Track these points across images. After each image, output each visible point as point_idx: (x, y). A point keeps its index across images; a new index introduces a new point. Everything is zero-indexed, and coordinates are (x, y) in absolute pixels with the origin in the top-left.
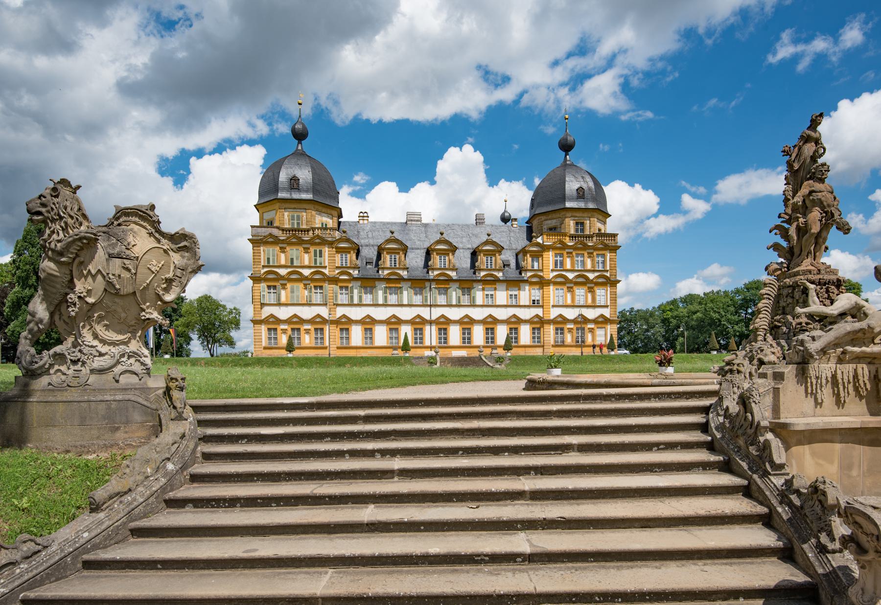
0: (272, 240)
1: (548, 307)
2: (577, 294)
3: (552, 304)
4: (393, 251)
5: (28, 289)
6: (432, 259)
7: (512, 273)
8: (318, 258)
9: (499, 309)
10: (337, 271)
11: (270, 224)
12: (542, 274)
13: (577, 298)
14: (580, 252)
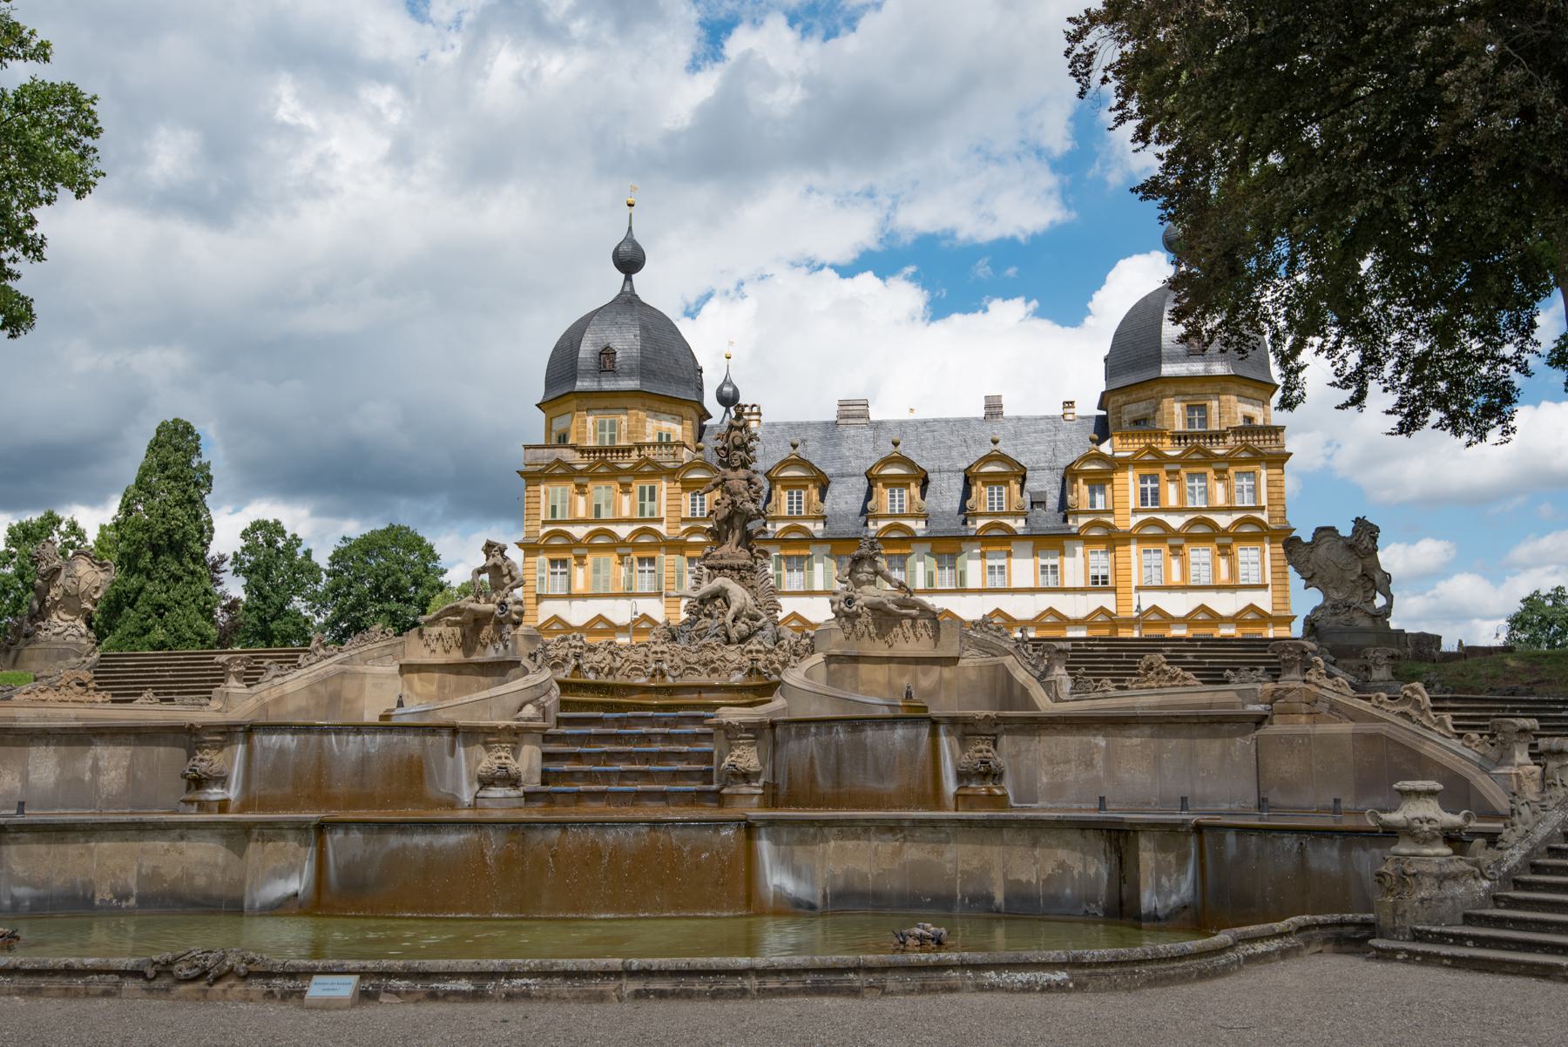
0: (562, 471)
1: (1125, 590)
2: (1192, 560)
3: (1135, 583)
5: (136, 576)
6: (875, 497)
7: (1047, 518)
8: (647, 503)
9: (1017, 597)
10: (683, 528)
11: (563, 439)
12: (1110, 520)
13: (1193, 569)
14: (1196, 470)
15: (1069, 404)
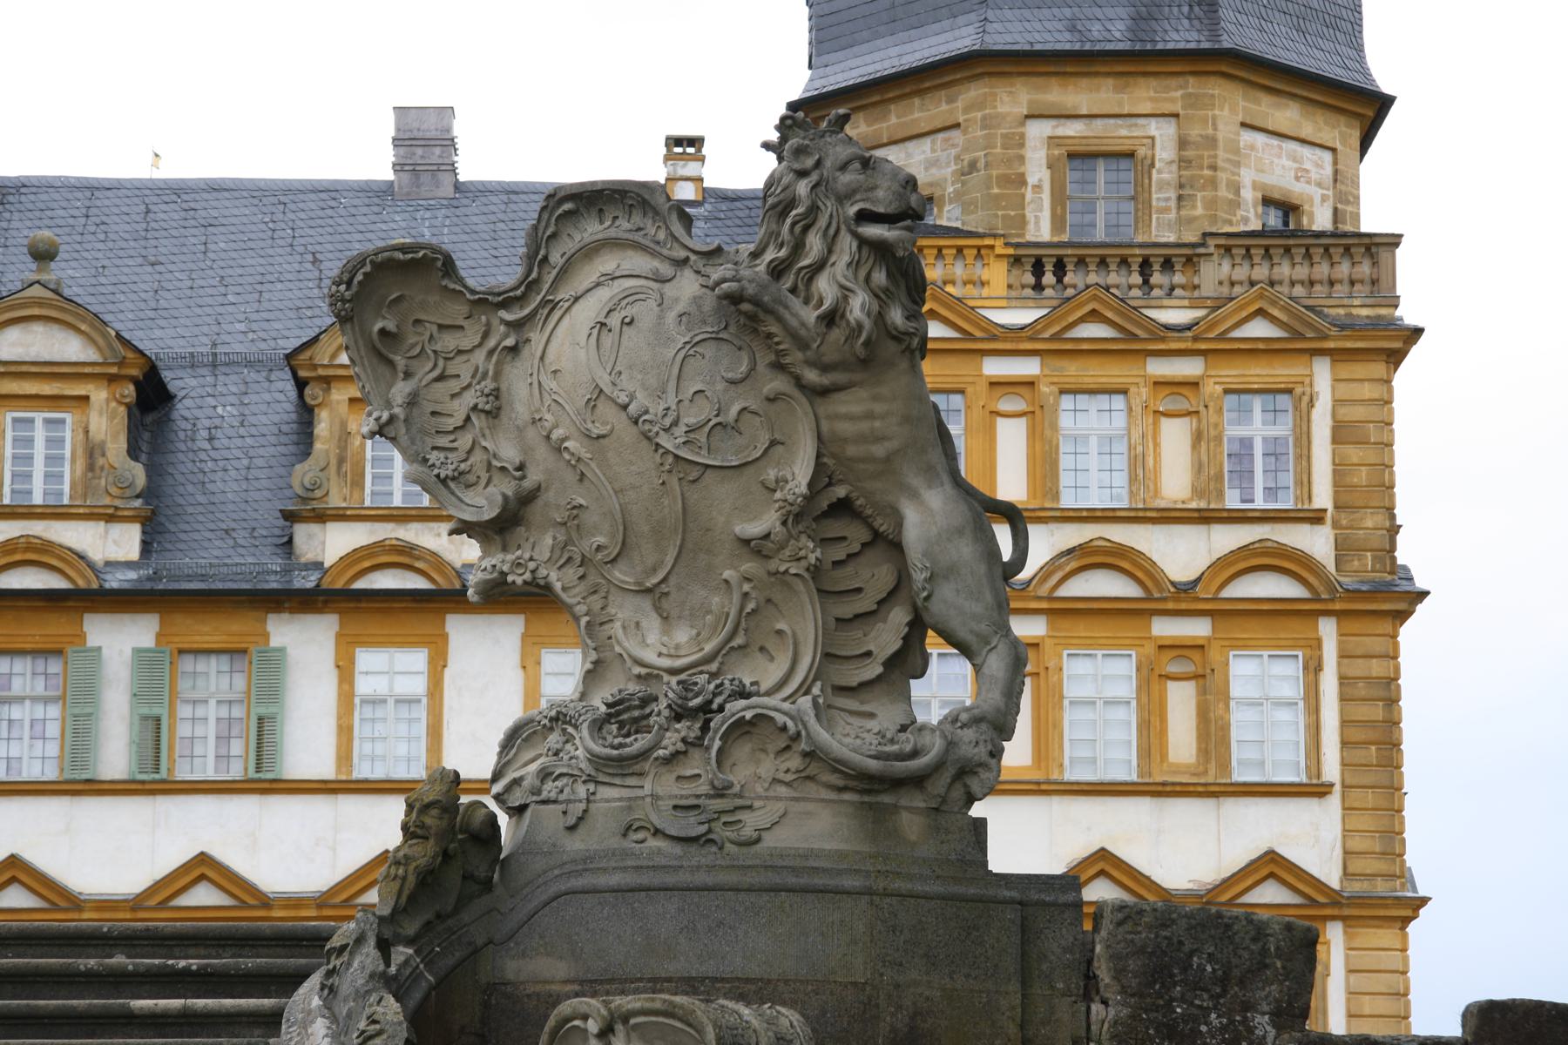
15: (685, 146)
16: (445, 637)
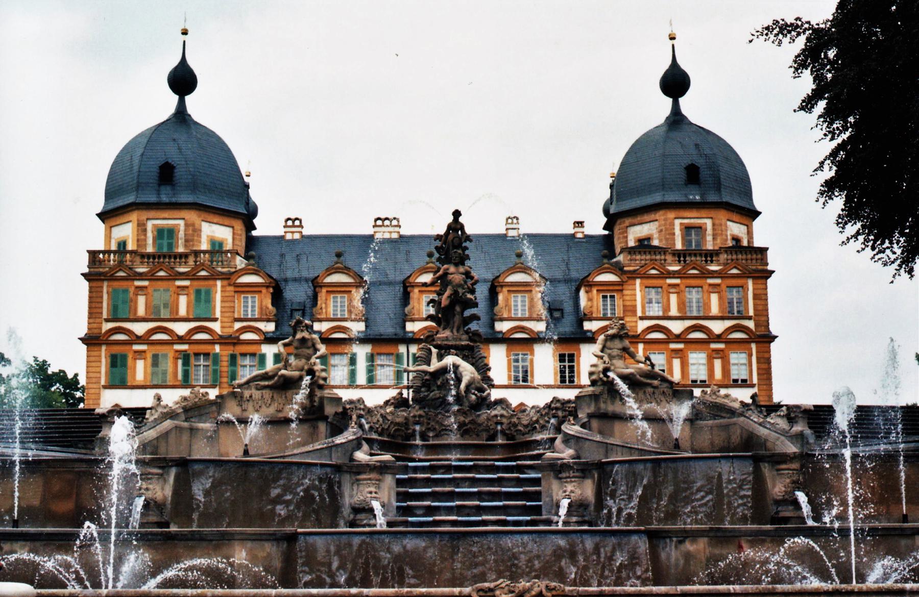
4: (339, 289)
10: (238, 325)
15: (579, 224)
16: (533, 350)
